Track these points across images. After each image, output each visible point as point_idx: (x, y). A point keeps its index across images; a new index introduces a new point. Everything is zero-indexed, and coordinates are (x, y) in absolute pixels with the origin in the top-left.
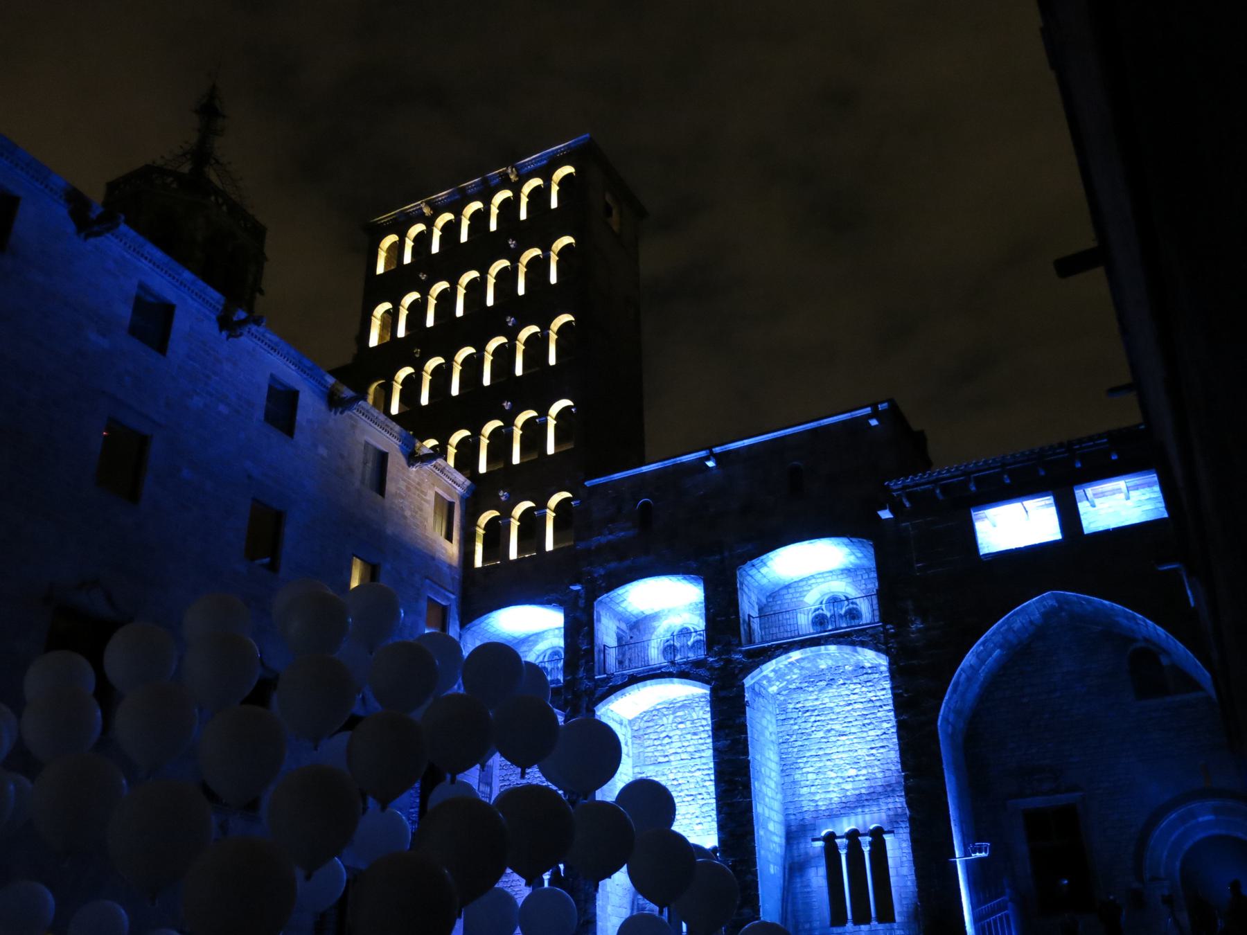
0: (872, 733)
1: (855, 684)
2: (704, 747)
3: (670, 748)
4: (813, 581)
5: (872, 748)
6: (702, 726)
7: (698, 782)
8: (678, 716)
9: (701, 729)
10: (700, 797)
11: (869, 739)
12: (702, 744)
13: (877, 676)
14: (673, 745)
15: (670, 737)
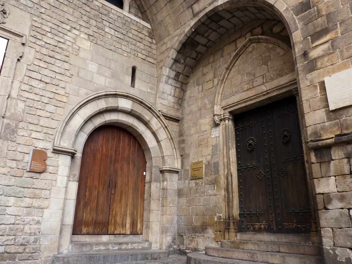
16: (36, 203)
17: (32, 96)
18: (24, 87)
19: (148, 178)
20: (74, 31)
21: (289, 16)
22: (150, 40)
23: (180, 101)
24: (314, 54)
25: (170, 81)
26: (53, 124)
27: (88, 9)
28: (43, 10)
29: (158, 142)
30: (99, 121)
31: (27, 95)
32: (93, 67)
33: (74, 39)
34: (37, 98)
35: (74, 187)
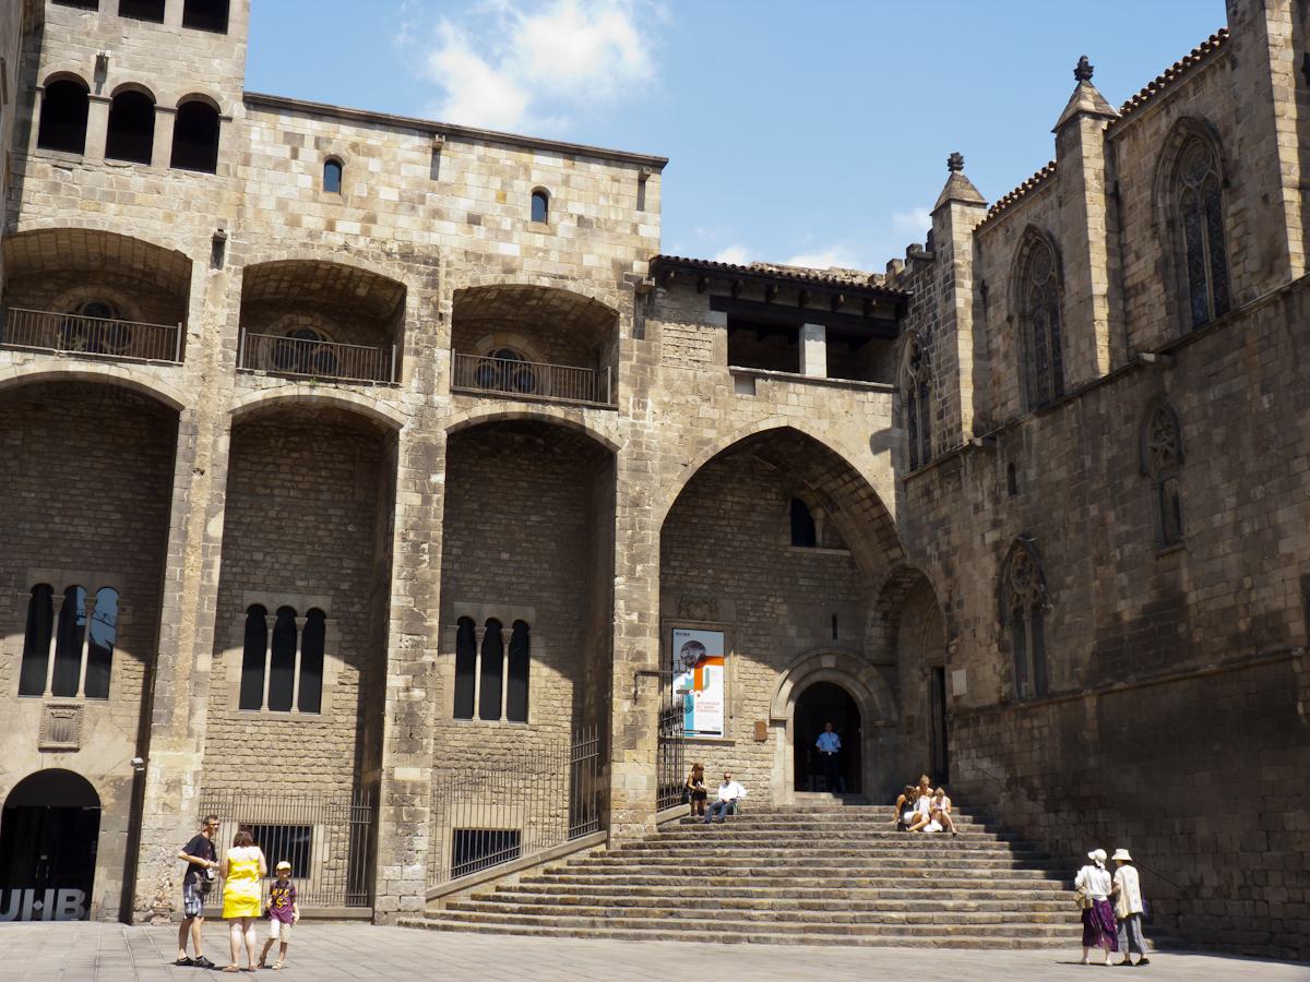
0: (533, 518)
1: (523, 459)
2: (323, 488)
3: (275, 479)
4: (490, 325)
5: (531, 535)
6: (326, 462)
7: (307, 528)
8: (294, 442)
9: (322, 464)
10: (308, 547)
11: (528, 523)
12: (322, 484)
13: (549, 456)
14: (281, 476)
15: (278, 466)
16: (764, 764)
17: (748, 676)
18: (742, 670)
19: (863, 735)
20: (772, 599)
21: (942, 608)
22: (851, 572)
23: (892, 641)
24: (952, 649)
25: (878, 623)
26: (767, 697)
27: (779, 567)
28: (742, 591)
29: (870, 694)
30: (804, 685)
31: (744, 676)
32: (792, 631)
33: (772, 608)
34: (752, 677)
35: (790, 749)
